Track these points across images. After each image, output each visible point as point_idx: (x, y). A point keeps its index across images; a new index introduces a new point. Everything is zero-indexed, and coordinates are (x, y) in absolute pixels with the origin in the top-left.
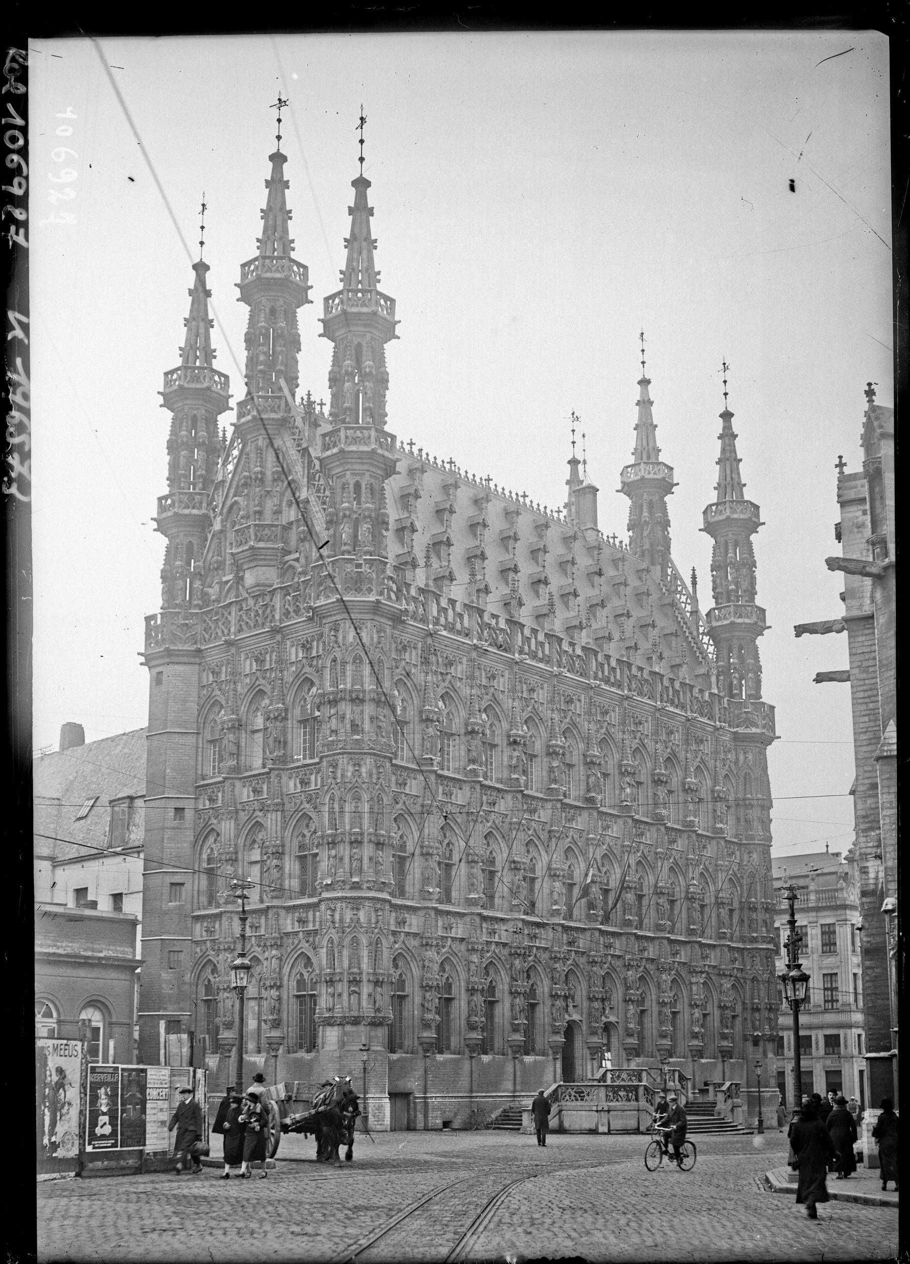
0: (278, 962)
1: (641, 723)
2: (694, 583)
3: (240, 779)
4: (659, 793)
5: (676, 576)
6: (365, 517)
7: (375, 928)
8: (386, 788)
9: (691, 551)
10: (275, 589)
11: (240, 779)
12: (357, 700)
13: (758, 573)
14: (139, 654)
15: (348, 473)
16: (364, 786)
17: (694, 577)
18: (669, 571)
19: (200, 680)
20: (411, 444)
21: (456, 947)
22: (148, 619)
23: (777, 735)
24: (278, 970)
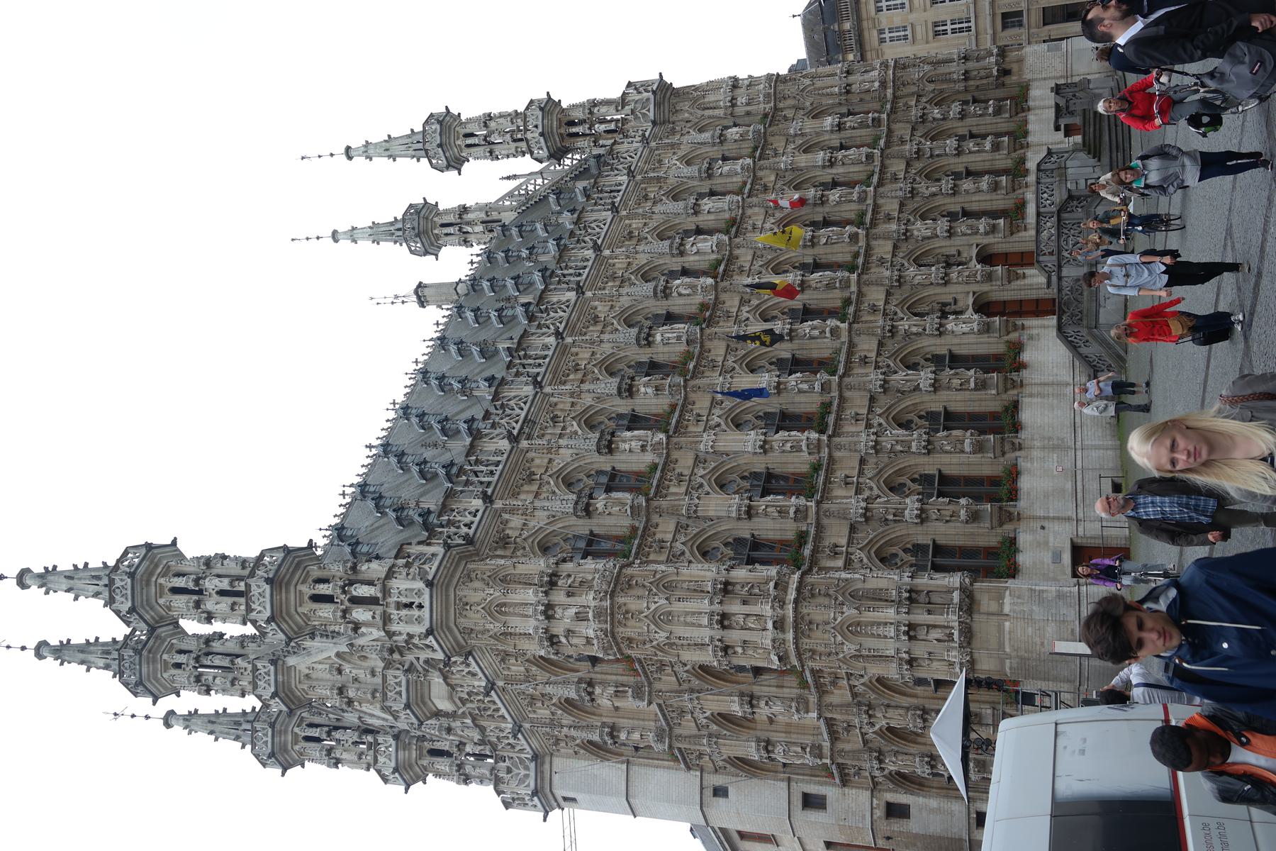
0: (890, 710)
1: (631, 232)
2: (515, 177)
3: (671, 729)
4: (707, 208)
5: (510, 195)
6: (344, 592)
7: (836, 599)
8: (658, 576)
9: (485, 182)
10: (448, 684)
11: (671, 729)
12: (549, 612)
13: (495, 111)
14: (545, 820)
15: (299, 610)
16: (653, 607)
17: (508, 178)
18: (507, 203)
19: (568, 757)
20: (344, 494)
21: (869, 472)
22: (507, 805)
23: (657, 77)
24: (901, 712)
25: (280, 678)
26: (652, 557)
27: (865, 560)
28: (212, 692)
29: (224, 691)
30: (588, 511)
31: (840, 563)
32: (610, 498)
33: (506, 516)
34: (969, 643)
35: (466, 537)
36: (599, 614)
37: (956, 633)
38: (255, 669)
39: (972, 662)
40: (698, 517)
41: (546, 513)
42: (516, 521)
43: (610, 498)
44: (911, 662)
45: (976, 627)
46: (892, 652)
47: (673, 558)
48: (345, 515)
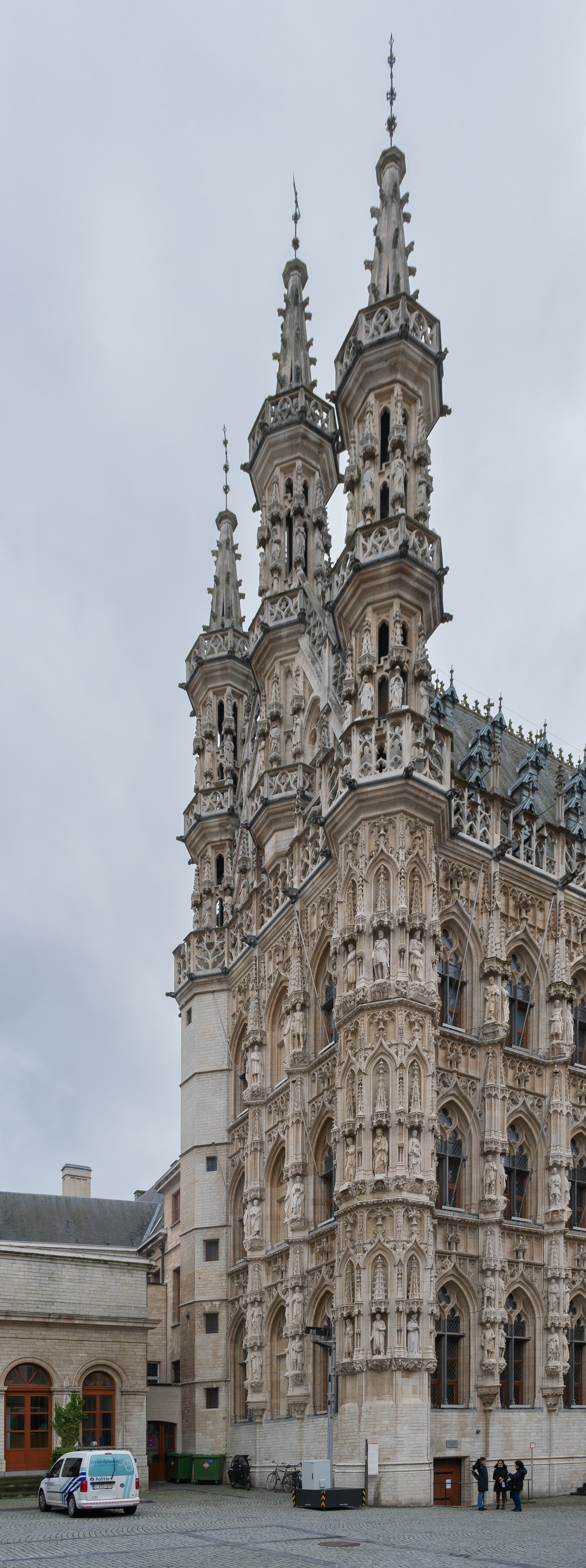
25: (284, 632)
26: (441, 1052)
27: (444, 1271)
28: (262, 550)
29: (264, 564)
30: (488, 976)
31: (440, 1247)
32: (503, 1000)
33: (481, 876)
34: (371, 1369)
35: (460, 828)
36: (382, 989)
37: (381, 1357)
38: (292, 594)
39: (353, 1373)
40: (484, 1098)
41: (485, 927)
42: (476, 892)
43: (503, 1000)
44: (350, 1318)
45: (387, 1375)
46: (358, 1298)
47: (442, 1075)
48: (466, 708)
